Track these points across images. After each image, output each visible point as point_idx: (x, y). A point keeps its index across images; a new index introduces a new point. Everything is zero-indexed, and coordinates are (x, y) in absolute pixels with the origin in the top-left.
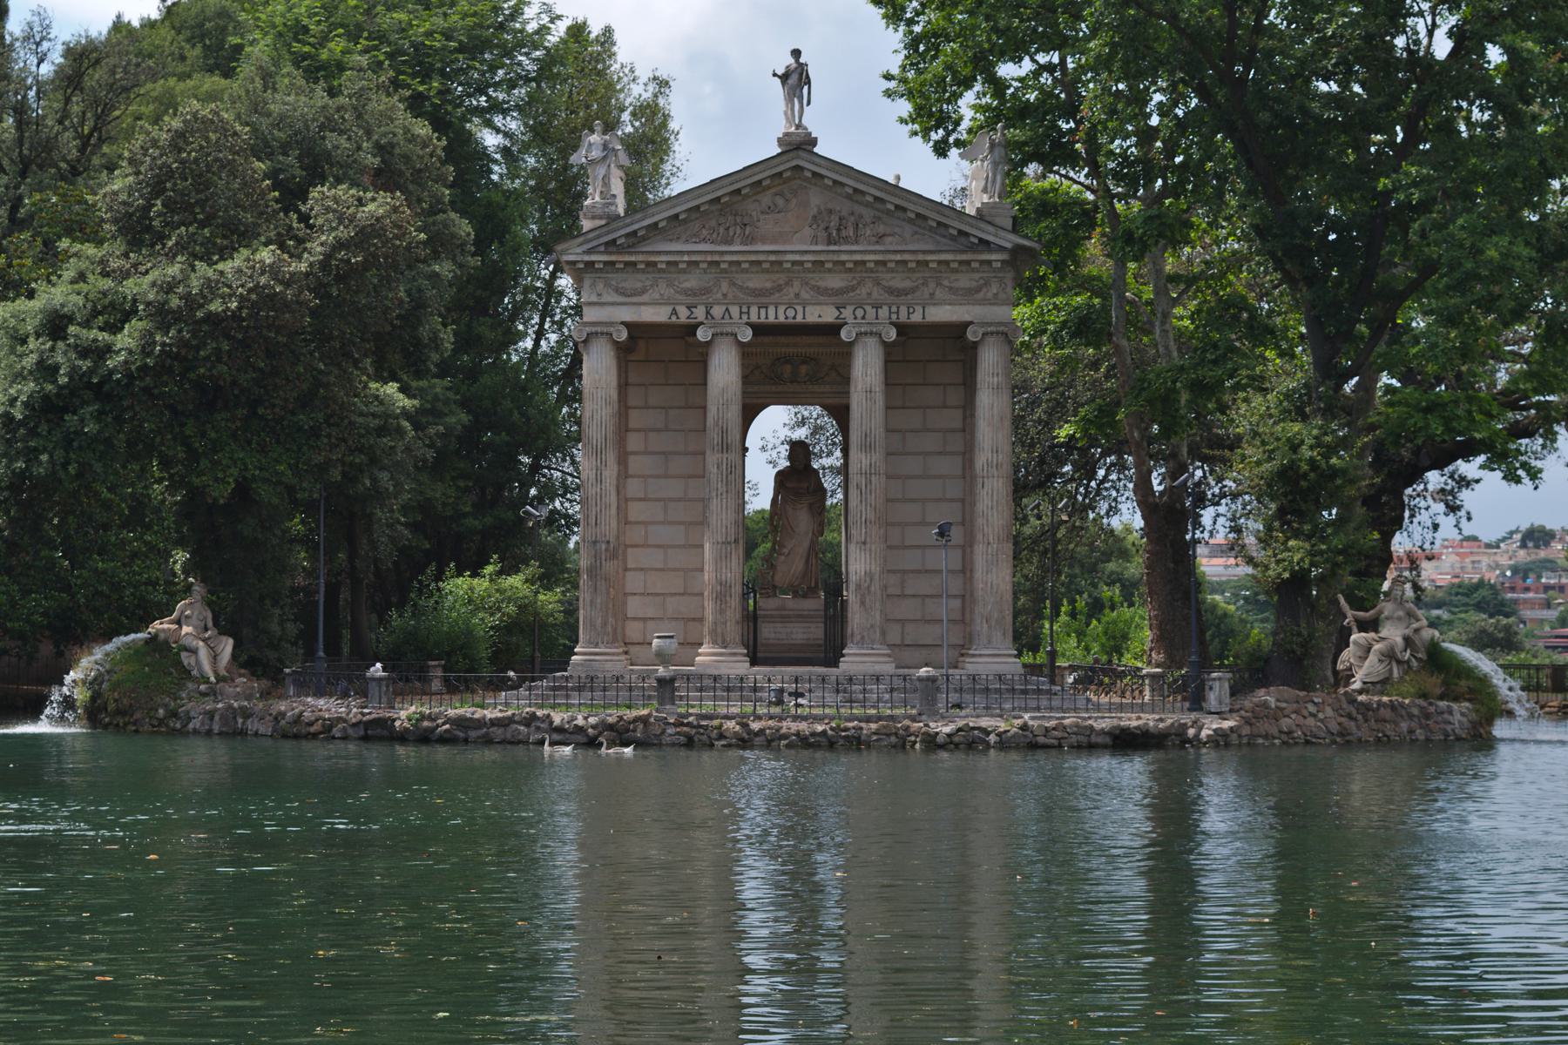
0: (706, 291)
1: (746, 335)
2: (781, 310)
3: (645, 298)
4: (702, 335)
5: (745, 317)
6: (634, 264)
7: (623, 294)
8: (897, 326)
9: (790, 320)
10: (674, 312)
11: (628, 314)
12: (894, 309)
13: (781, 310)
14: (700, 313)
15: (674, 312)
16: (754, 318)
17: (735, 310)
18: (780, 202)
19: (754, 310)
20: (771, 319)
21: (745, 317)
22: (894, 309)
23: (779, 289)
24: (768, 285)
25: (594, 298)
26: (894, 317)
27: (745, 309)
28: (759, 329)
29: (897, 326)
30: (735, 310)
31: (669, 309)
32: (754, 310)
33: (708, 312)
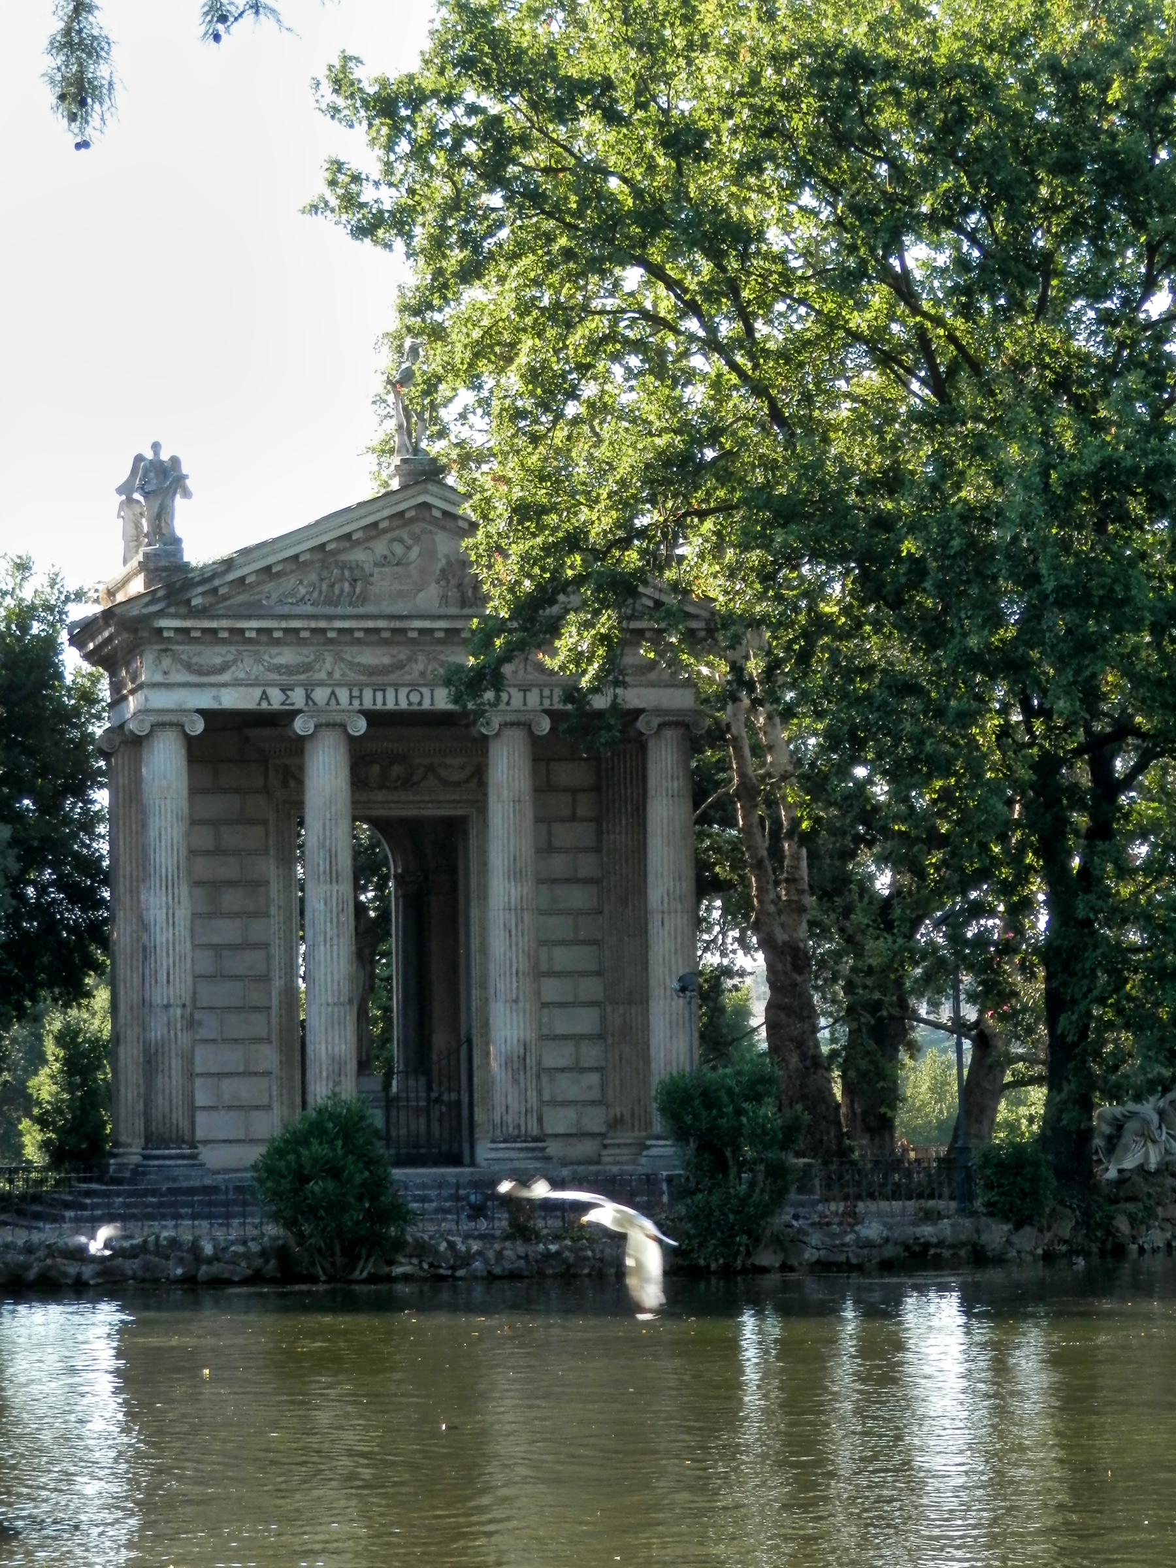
0: (307, 668)
1: (360, 726)
2: (403, 692)
3: (226, 677)
4: (301, 726)
5: (356, 703)
6: (214, 631)
7: (200, 672)
8: (548, 712)
9: (416, 707)
10: (265, 696)
11: (205, 700)
12: (546, 692)
13: (403, 692)
14: (298, 698)
15: (265, 696)
16: (368, 704)
17: (343, 695)
18: (398, 549)
19: (368, 694)
20: (390, 705)
21: (356, 703)
22: (546, 692)
23: (399, 666)
24: (386, 661)
25: (158, 678)
26: (547, 702)
27: (356, 693)
28: (374, 718)
29: (548, 712)
30: (343, 695)
31: (258, 692)
32: (368, 694)
33: (308, 697)
